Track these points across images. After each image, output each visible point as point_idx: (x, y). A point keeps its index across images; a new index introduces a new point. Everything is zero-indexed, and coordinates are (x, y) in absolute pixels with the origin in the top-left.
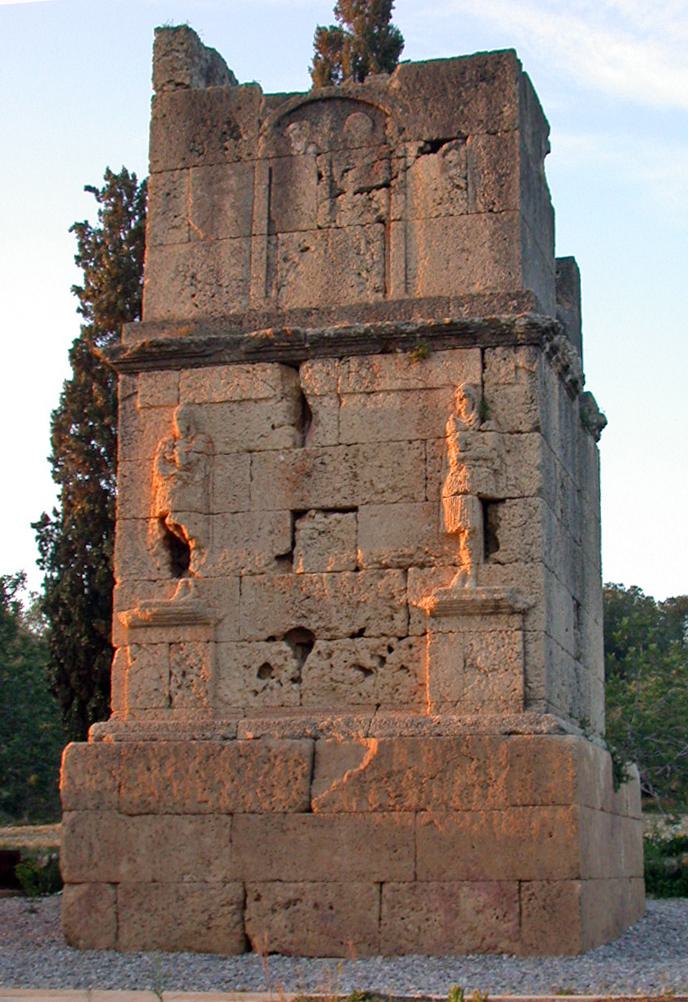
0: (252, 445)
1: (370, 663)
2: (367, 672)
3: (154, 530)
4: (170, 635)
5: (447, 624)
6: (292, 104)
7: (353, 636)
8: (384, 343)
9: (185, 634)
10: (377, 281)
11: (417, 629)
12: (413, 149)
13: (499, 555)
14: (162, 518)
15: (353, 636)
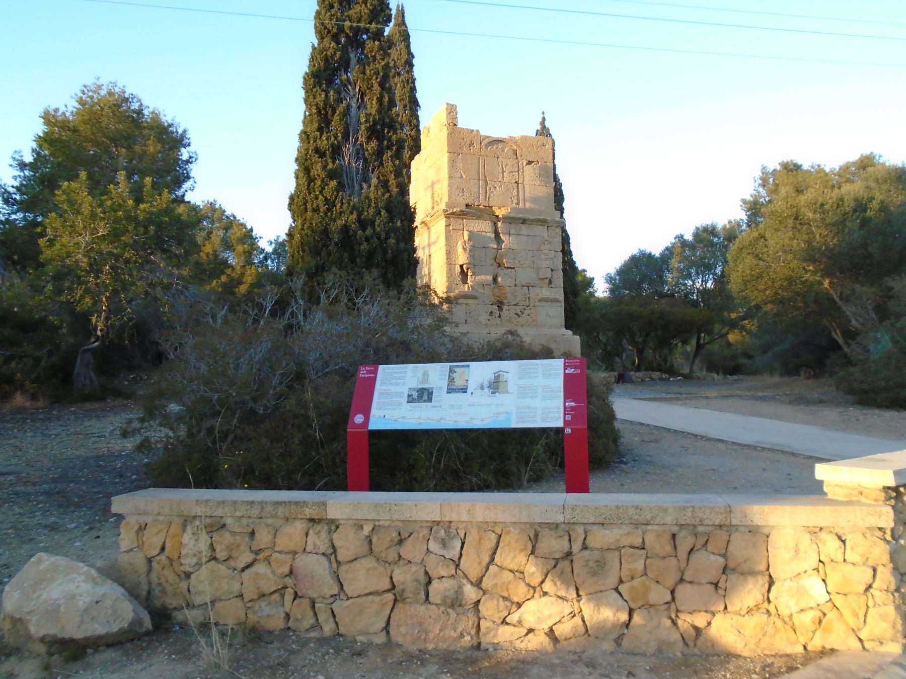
0: (486, 246)
1: (520, 313)
2: (519, 316)
3: (458, 269)
4: (465, 301)
5: (544, 304)
6: (490, 140)
7: (515, 305)
8: (524, 221)
9: (470, 301)
10: (516, 201)
11: (532, 304)
12: (525, 164)
13: (552, 286)
14: (461, 266)
15: (515, 305)
